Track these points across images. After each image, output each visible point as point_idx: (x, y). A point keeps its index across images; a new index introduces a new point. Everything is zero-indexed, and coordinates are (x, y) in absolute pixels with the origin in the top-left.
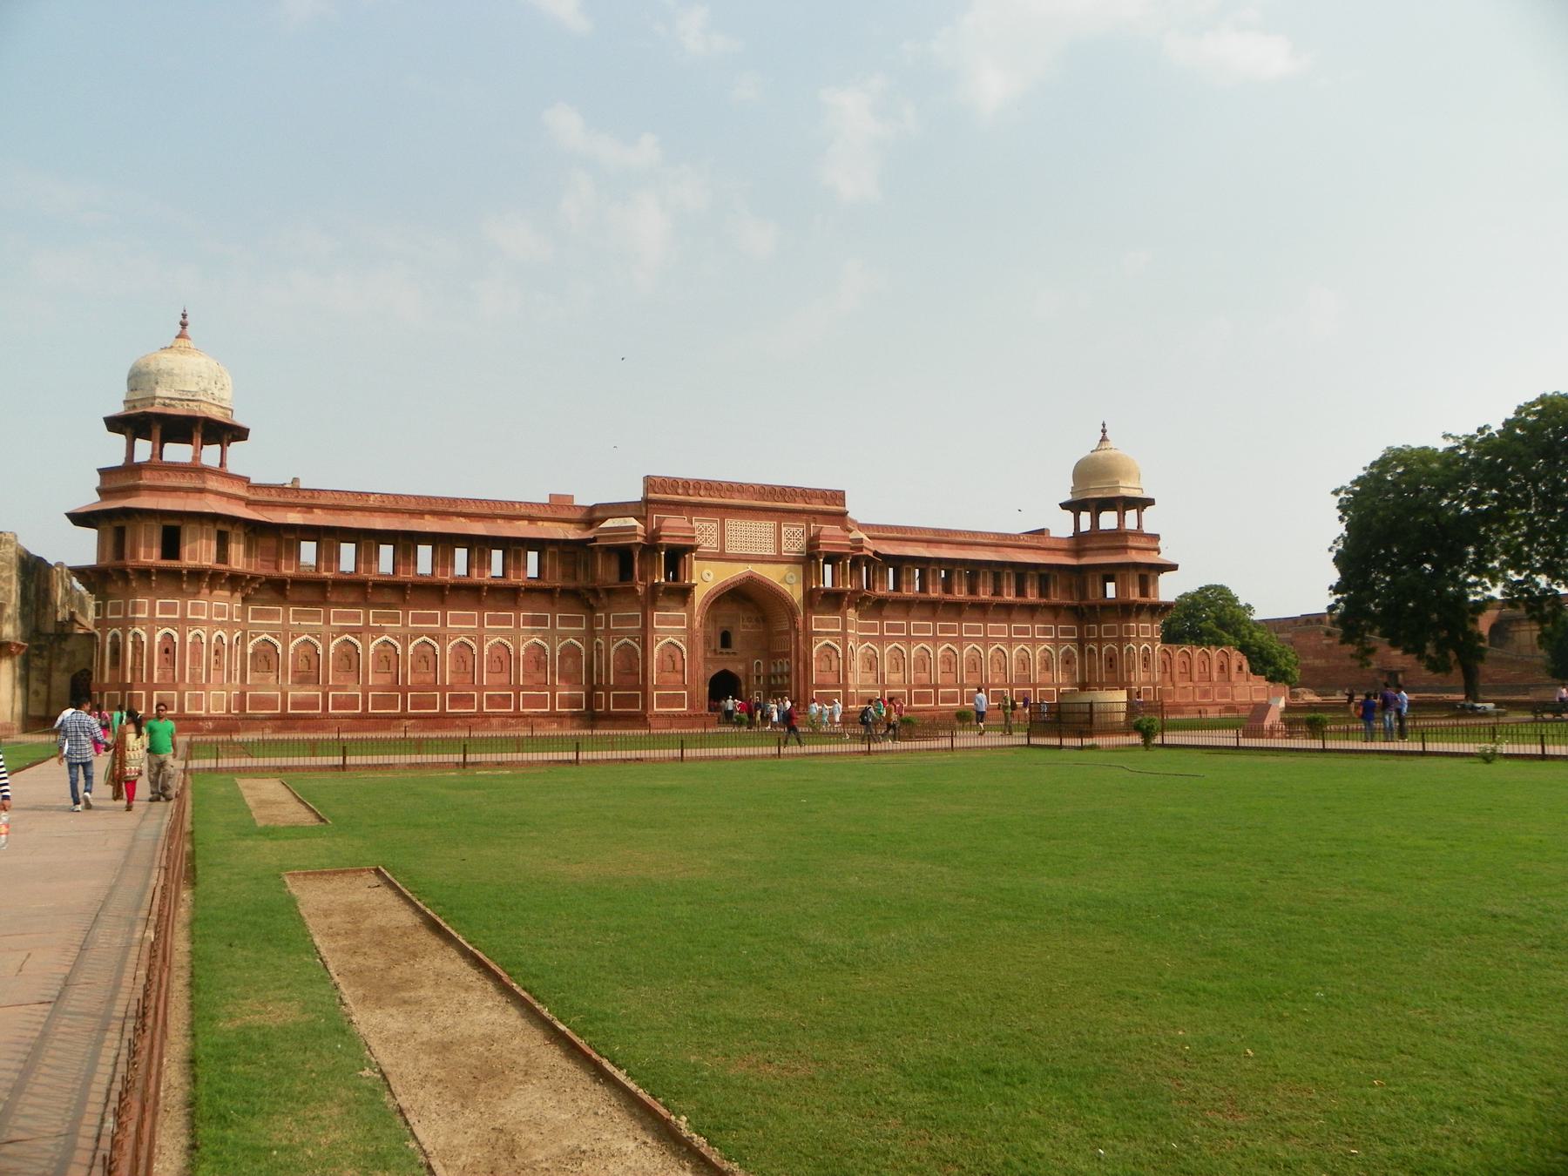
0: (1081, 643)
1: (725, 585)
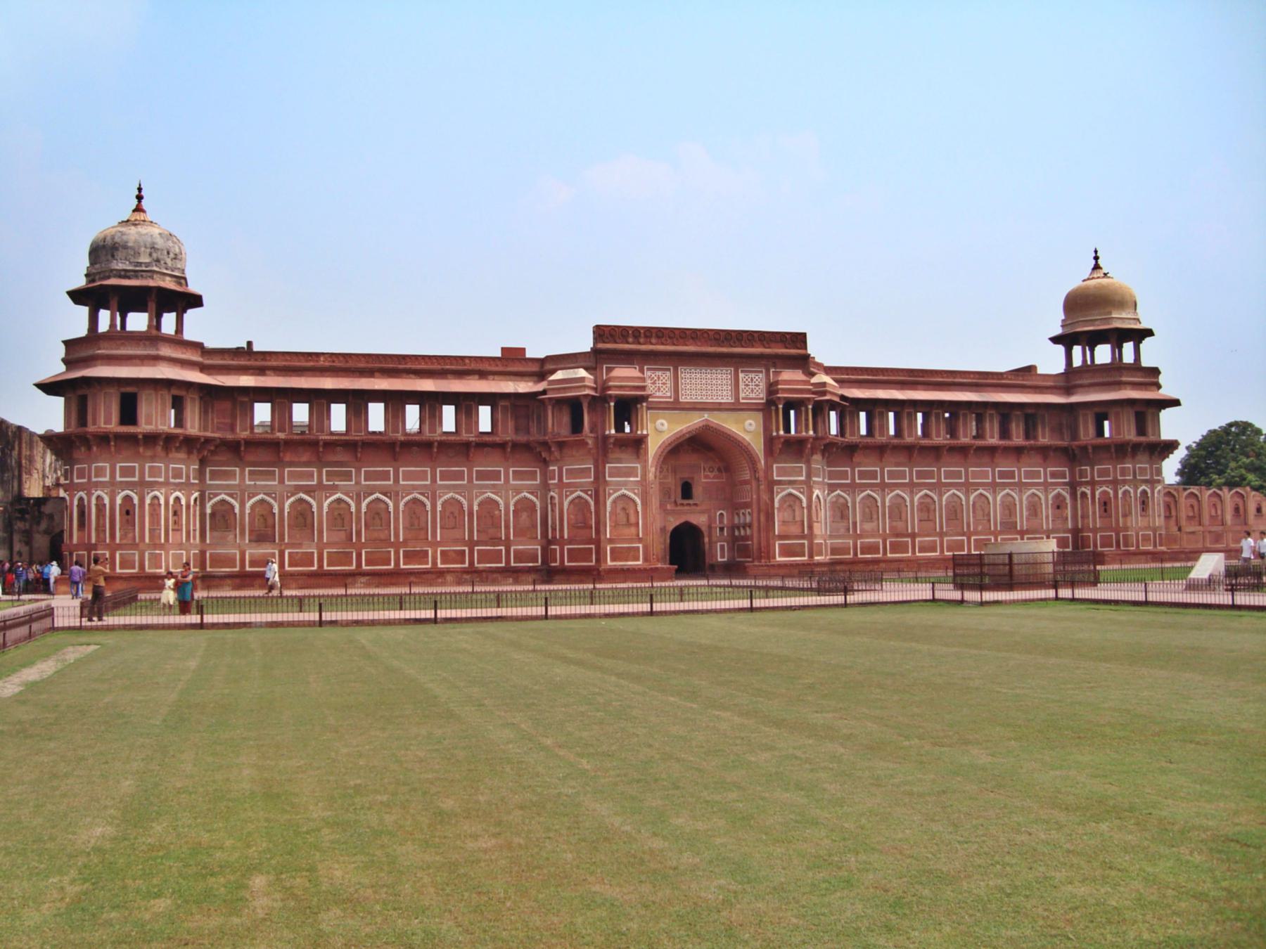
0: (1073, 486)
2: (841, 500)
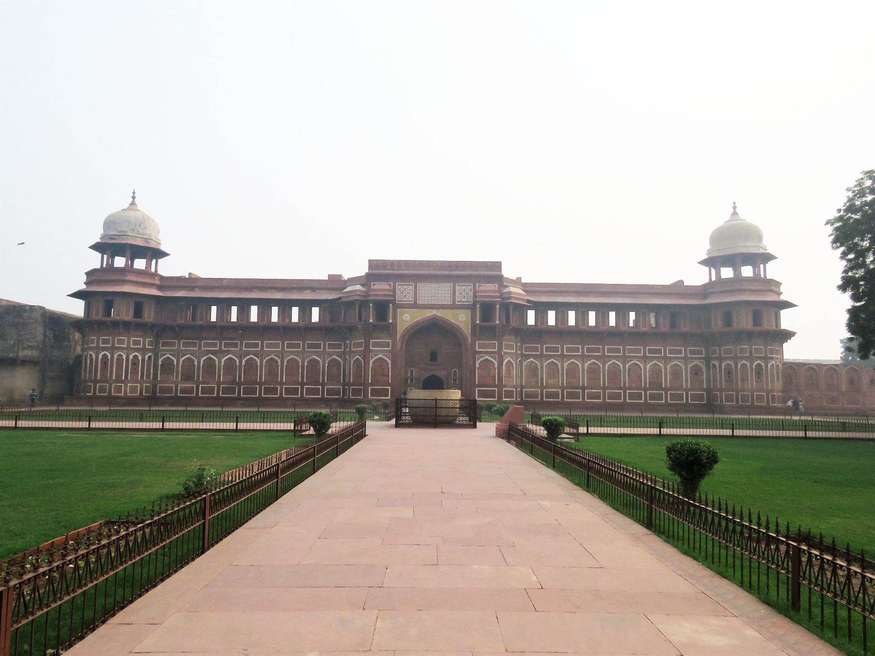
0: (707, 360)
1: (417, 324)
2: (533, 365)
